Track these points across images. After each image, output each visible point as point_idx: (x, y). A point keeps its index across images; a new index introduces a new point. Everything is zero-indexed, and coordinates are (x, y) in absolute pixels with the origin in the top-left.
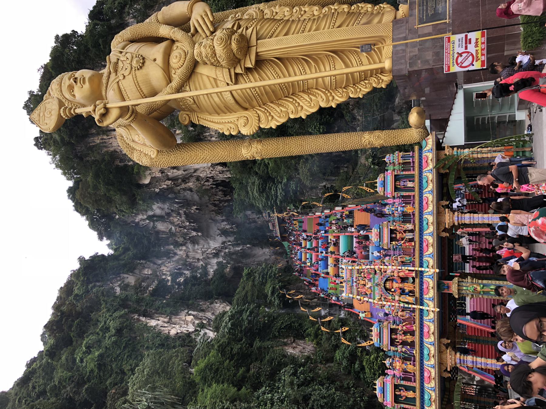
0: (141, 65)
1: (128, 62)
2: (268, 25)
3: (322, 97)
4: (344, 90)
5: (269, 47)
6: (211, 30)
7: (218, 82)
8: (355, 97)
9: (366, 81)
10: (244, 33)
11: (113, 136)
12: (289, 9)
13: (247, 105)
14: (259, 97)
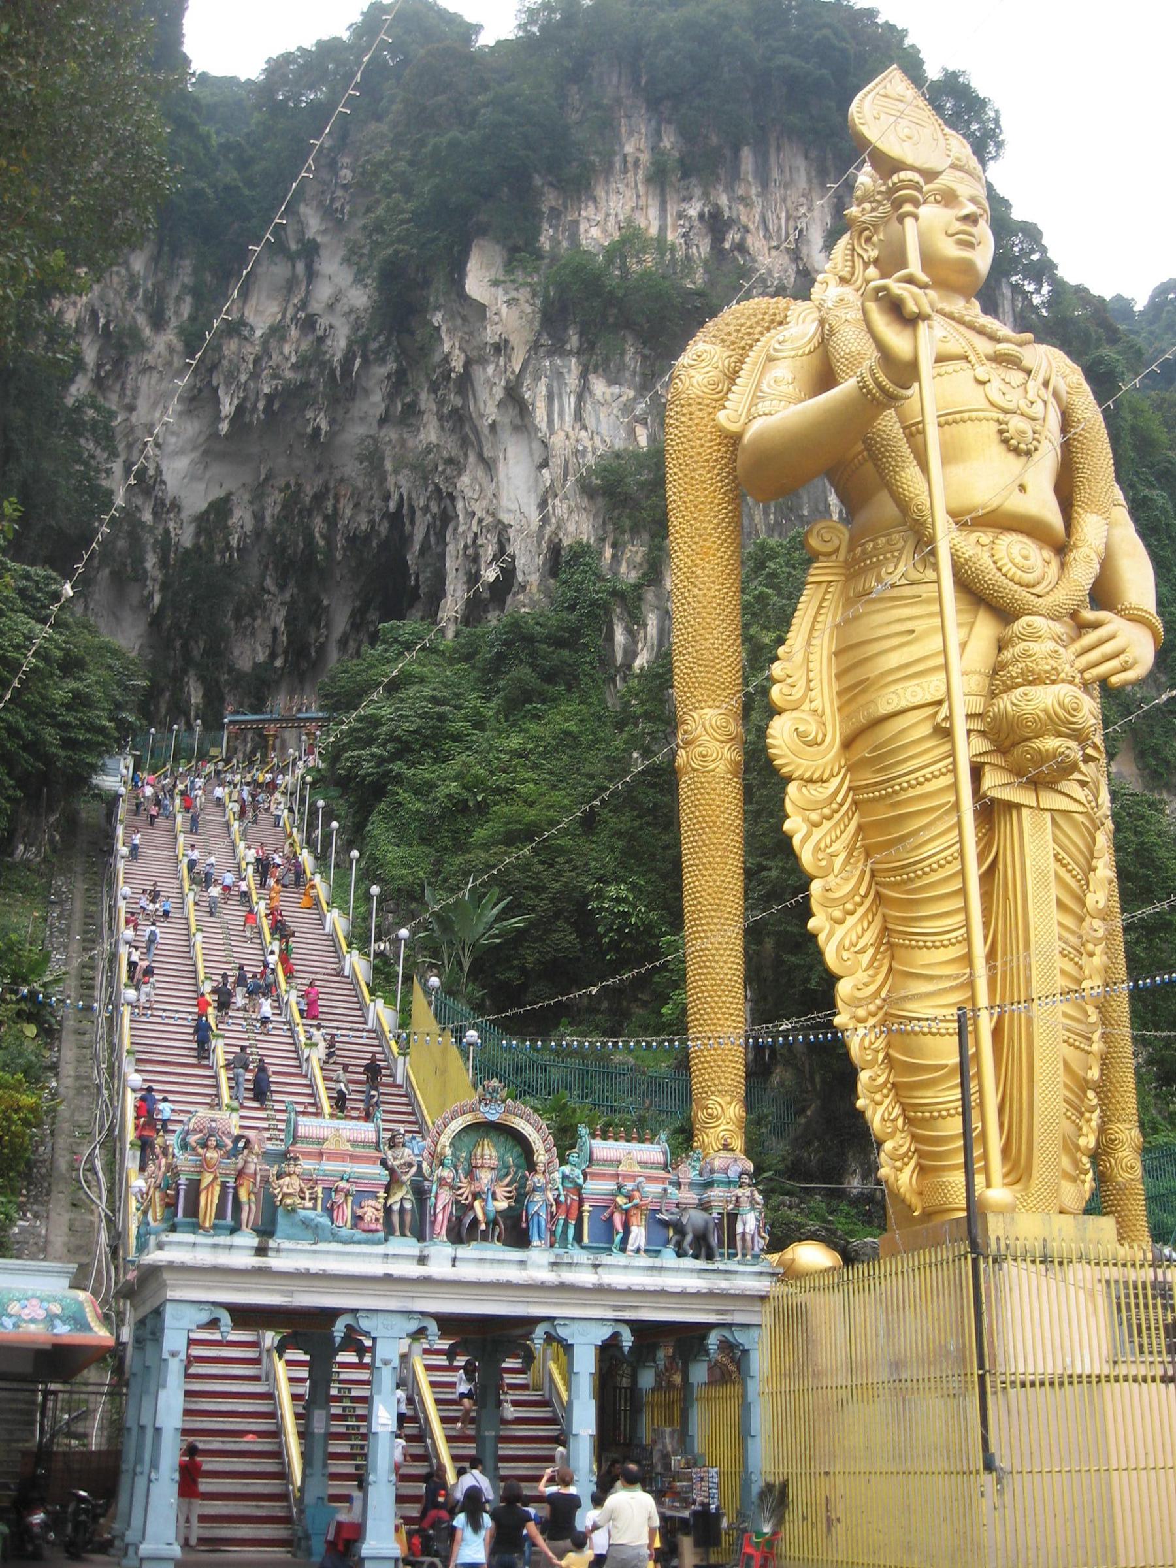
0: (1013, 442)
1: (1023, 405)
3: (866, 985)
4: (881, 1056)
8: (860, 1087)
9: (900, 1121)
10: (1076, 776)
11: (642, 202)
13: (862, 750)
14: (888, 795)
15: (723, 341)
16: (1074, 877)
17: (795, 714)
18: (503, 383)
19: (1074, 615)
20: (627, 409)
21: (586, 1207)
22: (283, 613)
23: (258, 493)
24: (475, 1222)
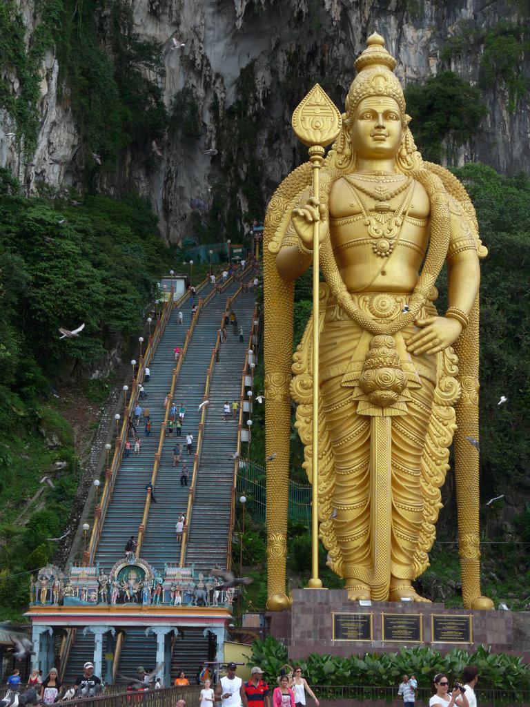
0: (379, 253)
5: (382, 433)
6: (416, 352)
7: (348, 362)
12: (445, 442)
16: (411, 439)
18: (360, 29)
19: (415, 323)
20: (426, 48)
21: (164, 590)
23: (273, 55)
24: (127, 597)
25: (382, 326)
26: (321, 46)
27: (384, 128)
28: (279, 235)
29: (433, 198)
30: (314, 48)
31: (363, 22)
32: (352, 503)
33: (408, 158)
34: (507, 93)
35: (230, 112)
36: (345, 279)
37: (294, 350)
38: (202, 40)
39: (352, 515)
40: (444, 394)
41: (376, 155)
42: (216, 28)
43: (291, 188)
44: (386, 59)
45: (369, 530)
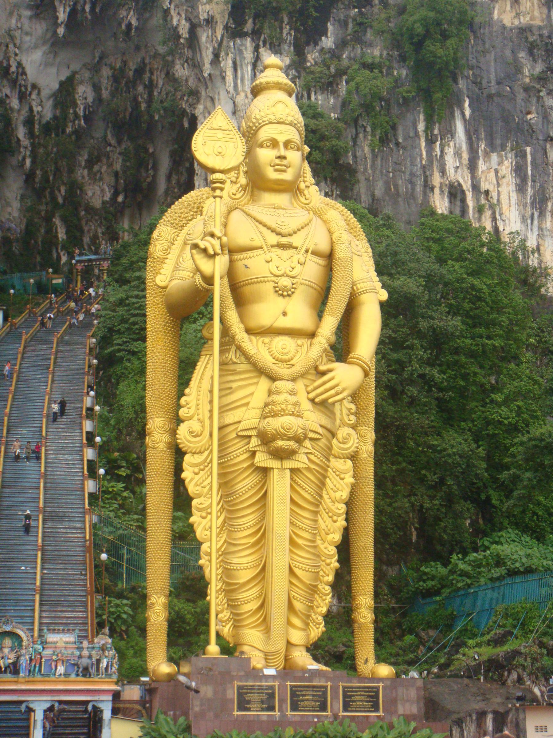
0: (280, 292)
2: (313, 479)
5: (280, 486)
6: (317, 400)
7: (244, 409)
9: (226, 605)
15: (172, 224)
16: (309, 494)
17: (191, 421)
18: (211, 49)
19: (316, 368)
21: (43, 660)
22: (120, 160)
25: (282, 371)
26: (150, 63)
27: (285, 158)
28: (167, 269)
29: (335, 236)
30: (142, 65)
31: (214, 42)
32: (244, 563)
33: (306, 192)
34: (369, 129)
35: (47, 128)
36: (242, 317)
37: (181, 394)
38: (18, 45)
39: (244, 576)
40: (342, 445)
41: (276, 187)
42: (34, 33)
43: (180, 217)
44: (286, 85)
45: (264, 592)
